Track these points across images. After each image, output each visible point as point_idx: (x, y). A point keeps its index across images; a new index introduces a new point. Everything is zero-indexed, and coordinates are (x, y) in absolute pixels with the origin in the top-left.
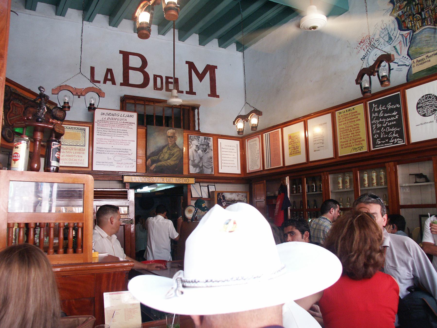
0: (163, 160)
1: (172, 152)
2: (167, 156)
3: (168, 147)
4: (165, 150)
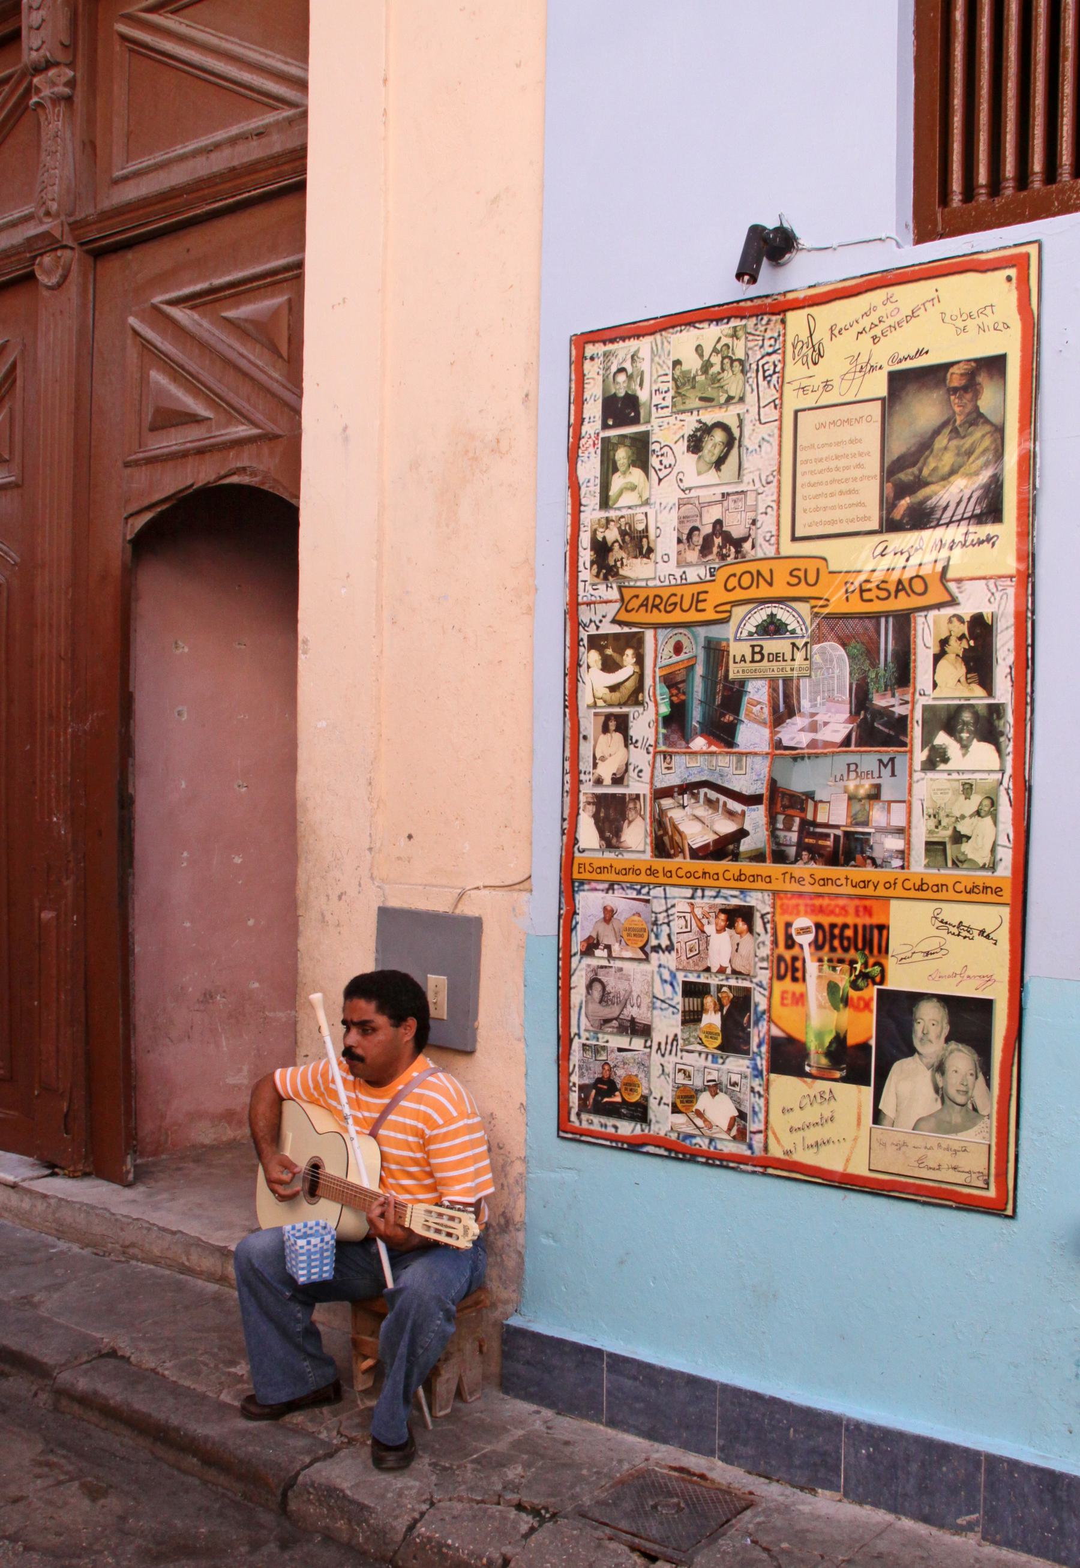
0: (934, 480)
1: (967, 446)
2: (948, 460)
3: (950, 428)
4: (941, 441)
